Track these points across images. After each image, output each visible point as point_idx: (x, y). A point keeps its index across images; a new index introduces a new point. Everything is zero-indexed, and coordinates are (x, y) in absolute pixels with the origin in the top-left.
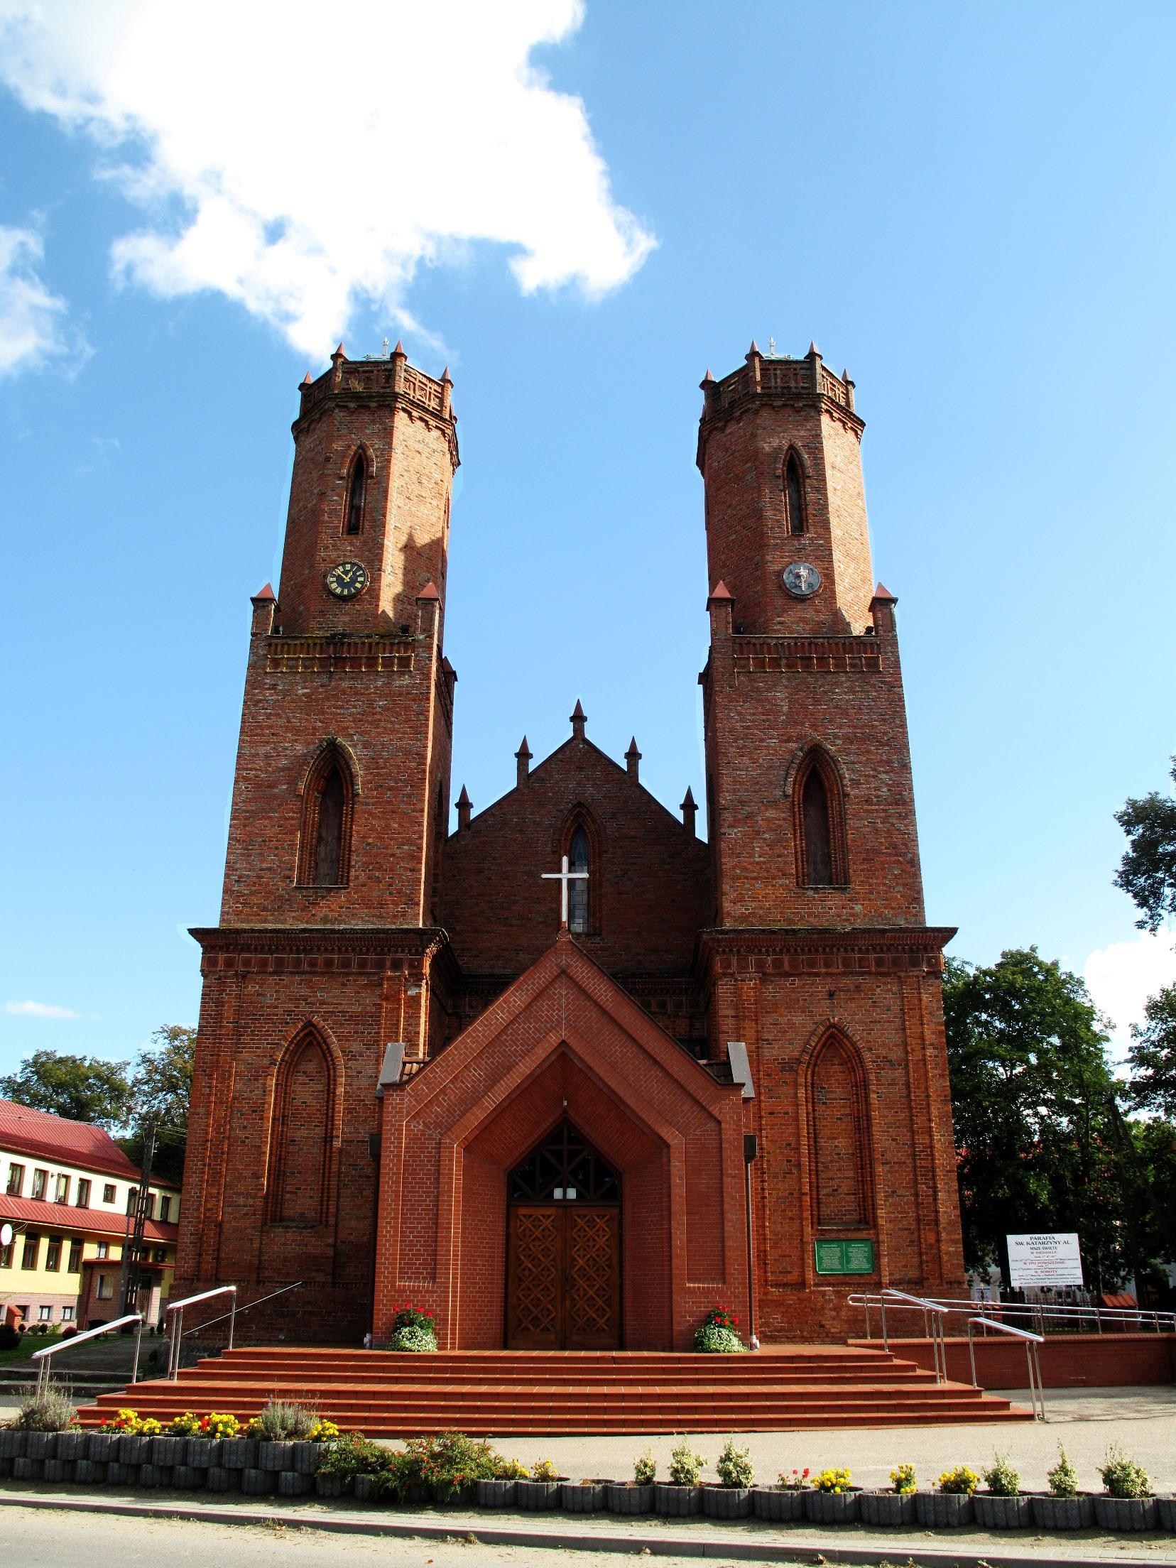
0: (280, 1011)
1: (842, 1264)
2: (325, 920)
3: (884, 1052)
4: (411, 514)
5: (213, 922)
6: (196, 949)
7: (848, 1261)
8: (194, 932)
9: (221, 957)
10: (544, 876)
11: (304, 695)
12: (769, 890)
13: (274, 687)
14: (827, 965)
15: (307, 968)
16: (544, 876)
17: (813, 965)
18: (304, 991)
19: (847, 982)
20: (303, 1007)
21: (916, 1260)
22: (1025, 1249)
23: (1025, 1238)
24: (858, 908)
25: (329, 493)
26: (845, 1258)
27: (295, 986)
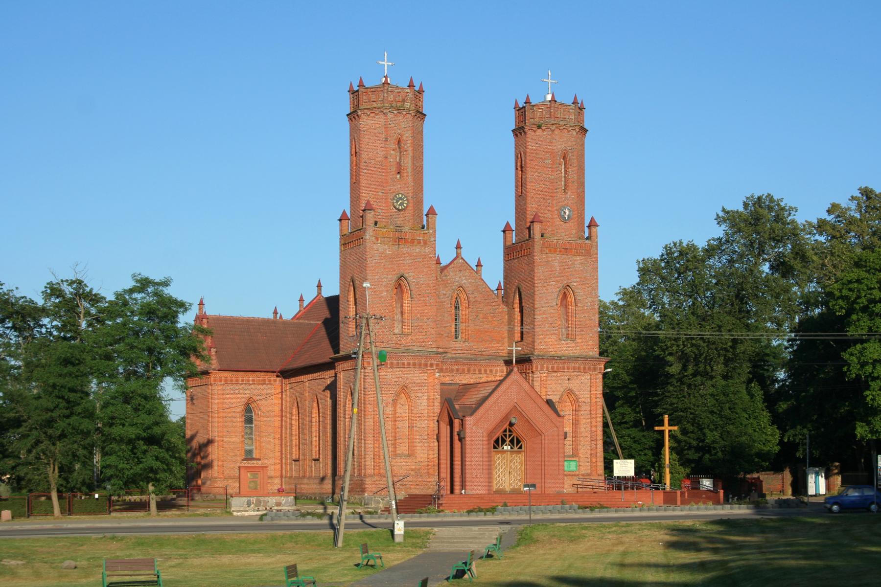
14: (568, 368)
27: (398, 372)
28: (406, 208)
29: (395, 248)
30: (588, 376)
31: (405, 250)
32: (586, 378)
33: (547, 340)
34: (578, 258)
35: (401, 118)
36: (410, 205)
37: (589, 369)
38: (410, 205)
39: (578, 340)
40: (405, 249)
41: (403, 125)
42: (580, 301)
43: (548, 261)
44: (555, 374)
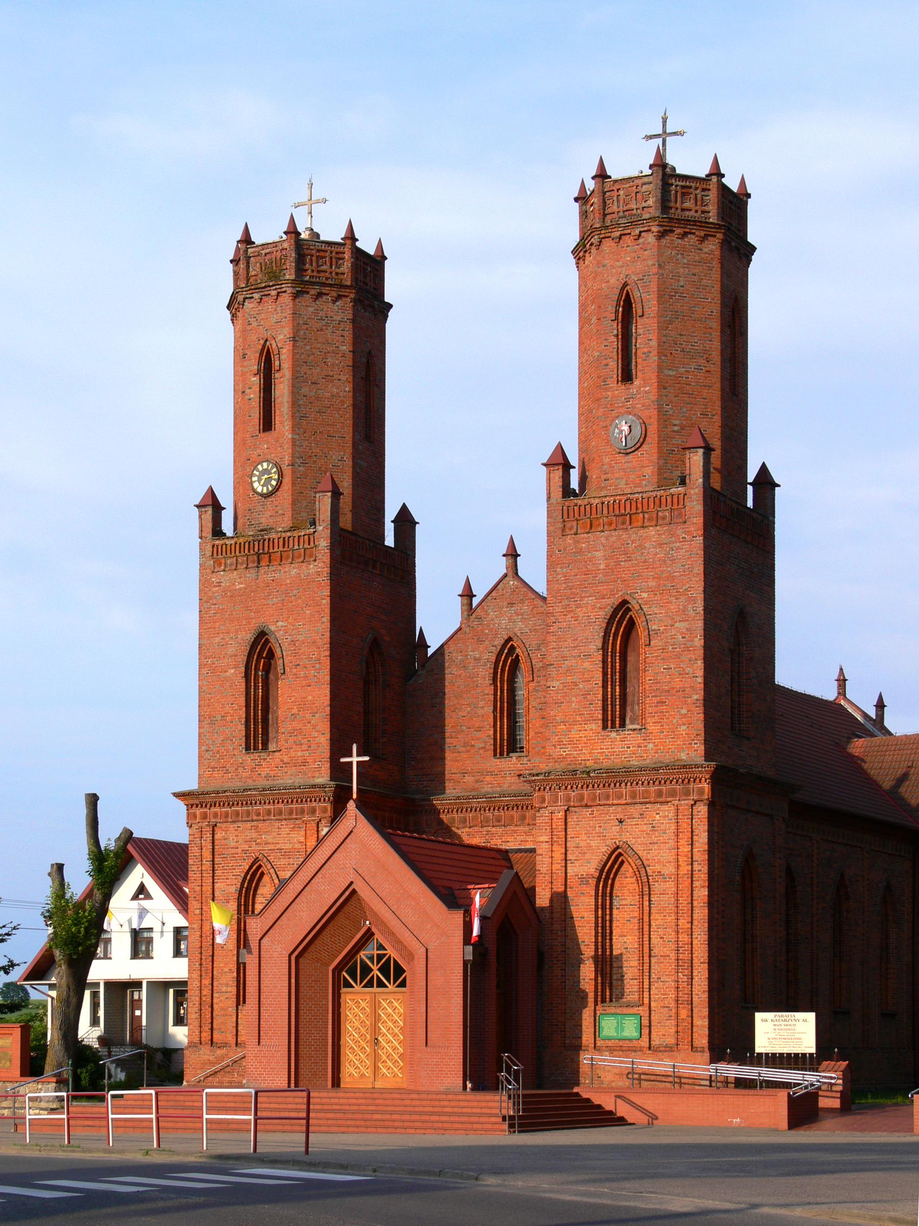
0: (239, 850)
1: (617, 1032)
2: (267, 777)
3: (658, 867)
4: (318, 398)
5: (192, 784)
6: (180, 807)
7: (623, 1030)
8: (177, 795)
9: (198, 811)
10: (750, 504)
11: (240, 589)
12: (582, 734)
13: (219, 584)
15: (255, 818)
16: (750, 504)
17: (608, 798)
18: (254, 835)
19: (634, 810)
20: (254, 847)
21: (673, 1030)
22: (769, 1026)
23: (770, 1015)
24: (651, 746)
25: (248, 391)
26: (620, 1027)
28: (277, 489)
29: (251, 575)
30: (668, 811)
31: (269, 577)
32: (663, 816)
33: (574, 734)
34: (652, 531)
35: (269, 305)
36: (287, 480)
37: (673, 793)
38: (287, 480)
39: (651, 727)
40: (268, 574)
41: (274, 318)
42: (657, 632)
43: (580, 551)
44: (587, 812)
